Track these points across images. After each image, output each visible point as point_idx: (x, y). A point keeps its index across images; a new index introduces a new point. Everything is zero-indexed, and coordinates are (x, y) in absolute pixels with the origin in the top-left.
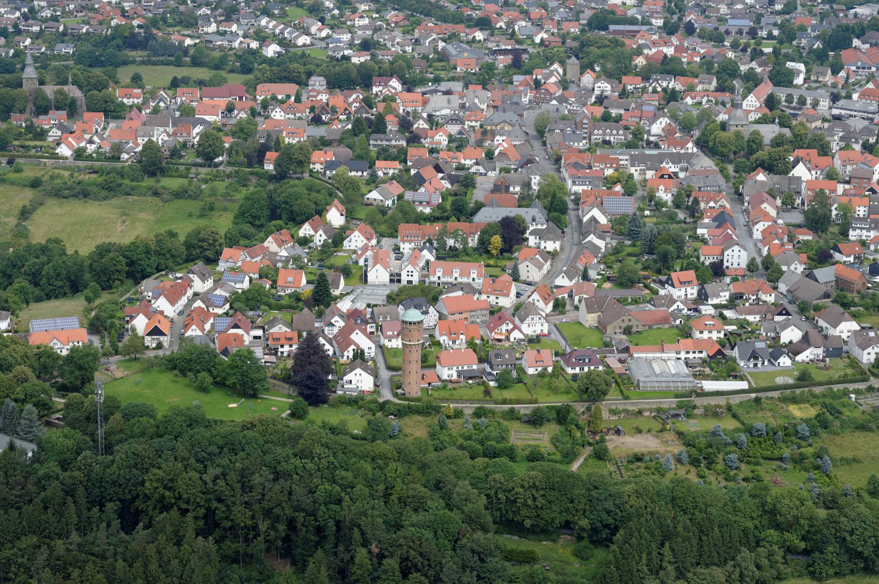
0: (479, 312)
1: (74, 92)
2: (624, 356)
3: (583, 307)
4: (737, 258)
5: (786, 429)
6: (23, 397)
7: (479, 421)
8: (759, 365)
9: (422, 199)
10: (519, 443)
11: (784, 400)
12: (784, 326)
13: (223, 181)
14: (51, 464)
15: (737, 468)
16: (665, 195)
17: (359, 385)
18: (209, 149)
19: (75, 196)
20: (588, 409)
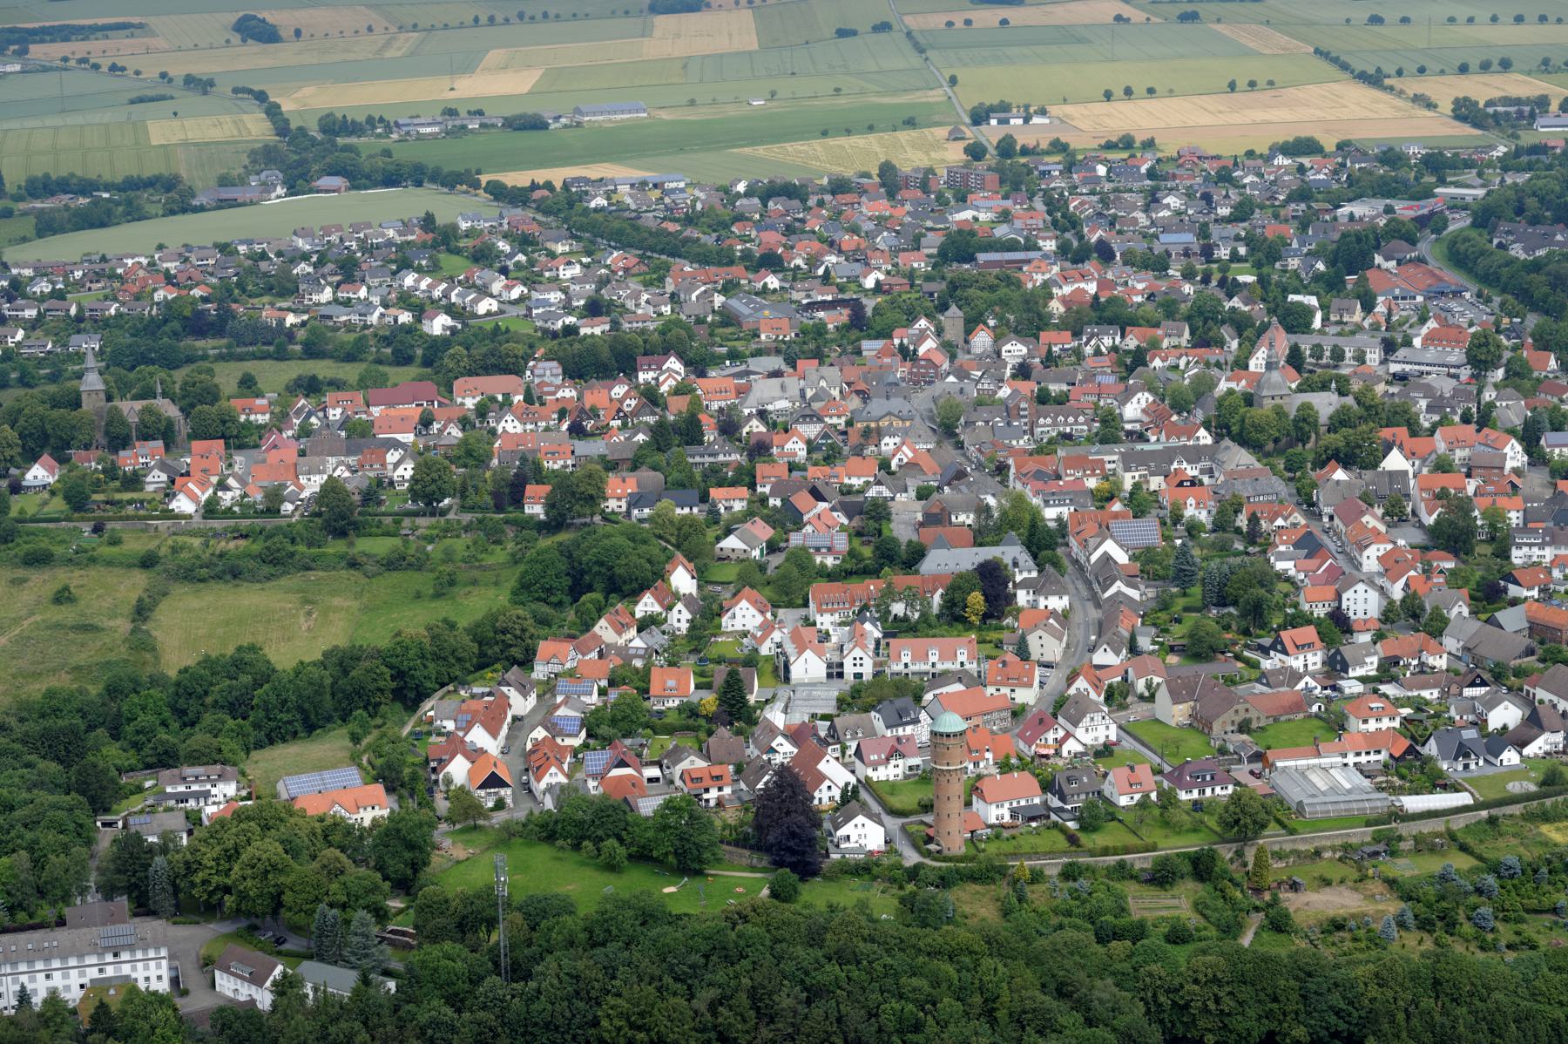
0: (996, 715)
1: (171, 410)
2: (1257, 767)
3: (1163, 695)
4: (1362, 603)
5: (1549, 862)
6: (345, 899)
7: (1076, 885)
8: (1473, 766)
9: (818, 544)
10: (1146, 914)
11: (1529, 817)
12: (1491, 704)
13: (458, 536)
14: (435, 1003)
15: (1492, 930)
16: (1196, 511)
17: (863, 842)
18: (433, 487)
19: (218, 577)
20: (1239, 854)
